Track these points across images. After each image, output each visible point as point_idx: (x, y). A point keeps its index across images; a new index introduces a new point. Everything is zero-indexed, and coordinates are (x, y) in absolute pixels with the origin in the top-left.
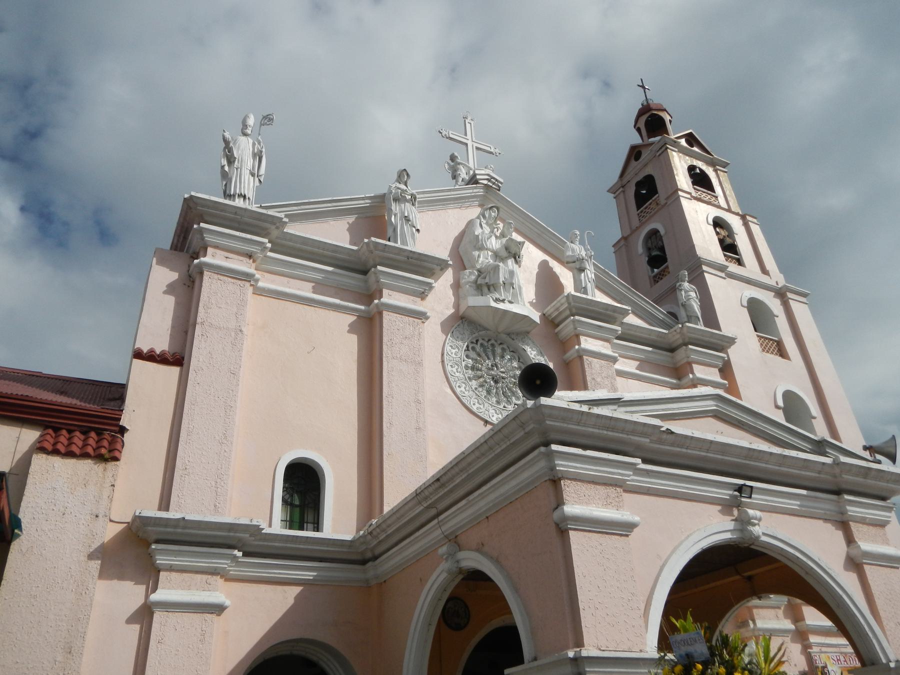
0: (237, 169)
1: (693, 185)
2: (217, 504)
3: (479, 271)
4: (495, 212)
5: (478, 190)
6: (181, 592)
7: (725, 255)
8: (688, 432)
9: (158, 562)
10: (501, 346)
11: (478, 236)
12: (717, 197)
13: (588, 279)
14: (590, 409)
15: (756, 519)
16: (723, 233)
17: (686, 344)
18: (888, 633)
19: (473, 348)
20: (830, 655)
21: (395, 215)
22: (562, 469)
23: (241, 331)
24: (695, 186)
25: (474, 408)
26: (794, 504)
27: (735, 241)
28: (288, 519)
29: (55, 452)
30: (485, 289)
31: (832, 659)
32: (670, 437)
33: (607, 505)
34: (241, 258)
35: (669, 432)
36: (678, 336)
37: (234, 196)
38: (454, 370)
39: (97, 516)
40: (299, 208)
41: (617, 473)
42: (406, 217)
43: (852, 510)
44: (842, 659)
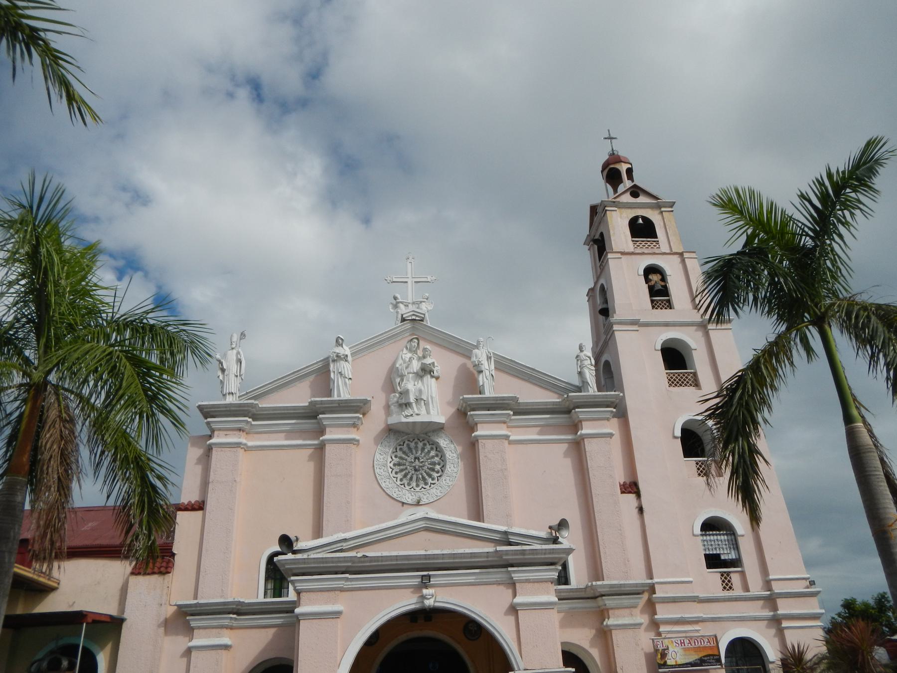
0: (227, 375)
1: (632, 238)
2: (223, 589)
3: (401, 393)
4: (415, 342)
5: (405, 326)
6: (204, 640)
7: (652, 301)
8: (378, 554)
9: (192, 625)
10: (422, 443)
11: (398, 367)
12: (658, 241)
13: (486, 377)
14: (308, 556)
15: (429, 595)
16: (655, 278)
17: (574, 408)
18: (523, 653)
19: (401, 449)
20: (674, 640)
21: (334, 372)
22: (299, 588)
23: (235, 481)
24: (633, 239)
25: (395, 496)
26: (471, 579)
27: (668, 283)
28: (273, 588)
29: (139, 574)
30: (404, 406)
31: (678, 644)
32: (366, 559)
33: (326, 603)
34: (235, 432)
35: (365, 556)
36: (567, 402)
37: (226, 394)
38: (382, 471)
39: (161, 605)
40: (273, 384)
41: (341, 584)
42: (340, 372)
43: (516, 576)
44: (686, 641)
